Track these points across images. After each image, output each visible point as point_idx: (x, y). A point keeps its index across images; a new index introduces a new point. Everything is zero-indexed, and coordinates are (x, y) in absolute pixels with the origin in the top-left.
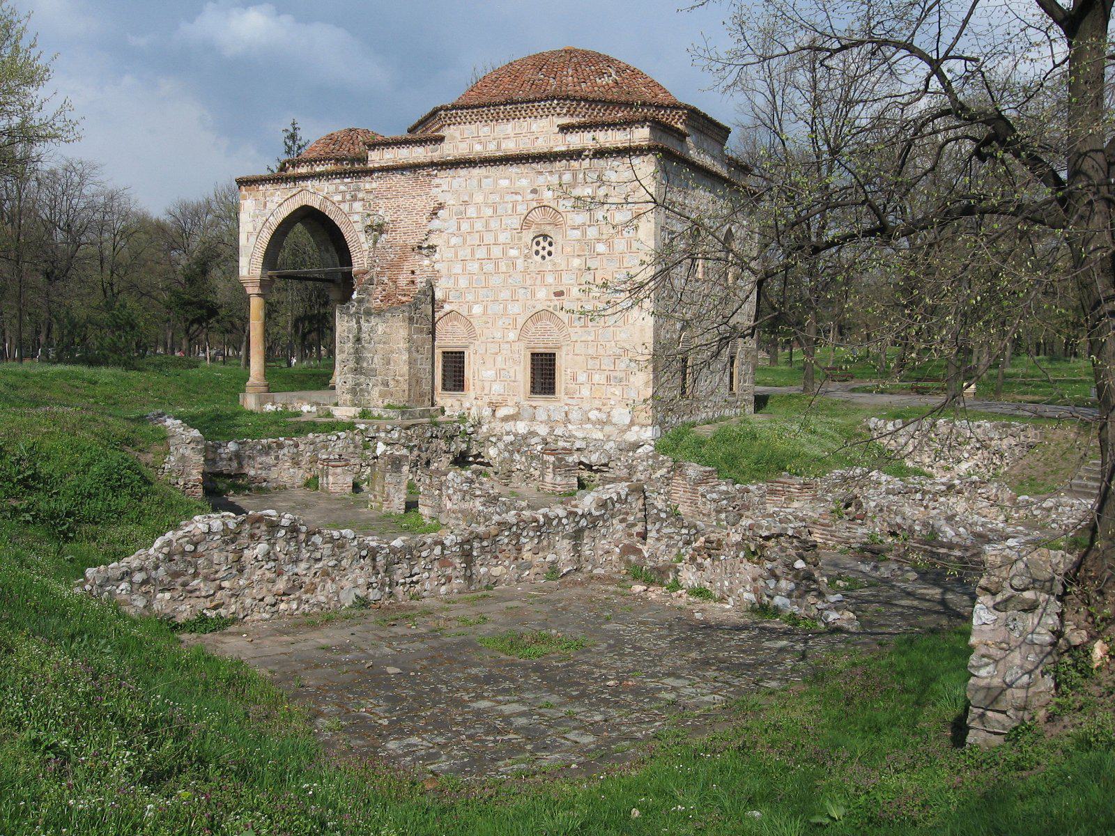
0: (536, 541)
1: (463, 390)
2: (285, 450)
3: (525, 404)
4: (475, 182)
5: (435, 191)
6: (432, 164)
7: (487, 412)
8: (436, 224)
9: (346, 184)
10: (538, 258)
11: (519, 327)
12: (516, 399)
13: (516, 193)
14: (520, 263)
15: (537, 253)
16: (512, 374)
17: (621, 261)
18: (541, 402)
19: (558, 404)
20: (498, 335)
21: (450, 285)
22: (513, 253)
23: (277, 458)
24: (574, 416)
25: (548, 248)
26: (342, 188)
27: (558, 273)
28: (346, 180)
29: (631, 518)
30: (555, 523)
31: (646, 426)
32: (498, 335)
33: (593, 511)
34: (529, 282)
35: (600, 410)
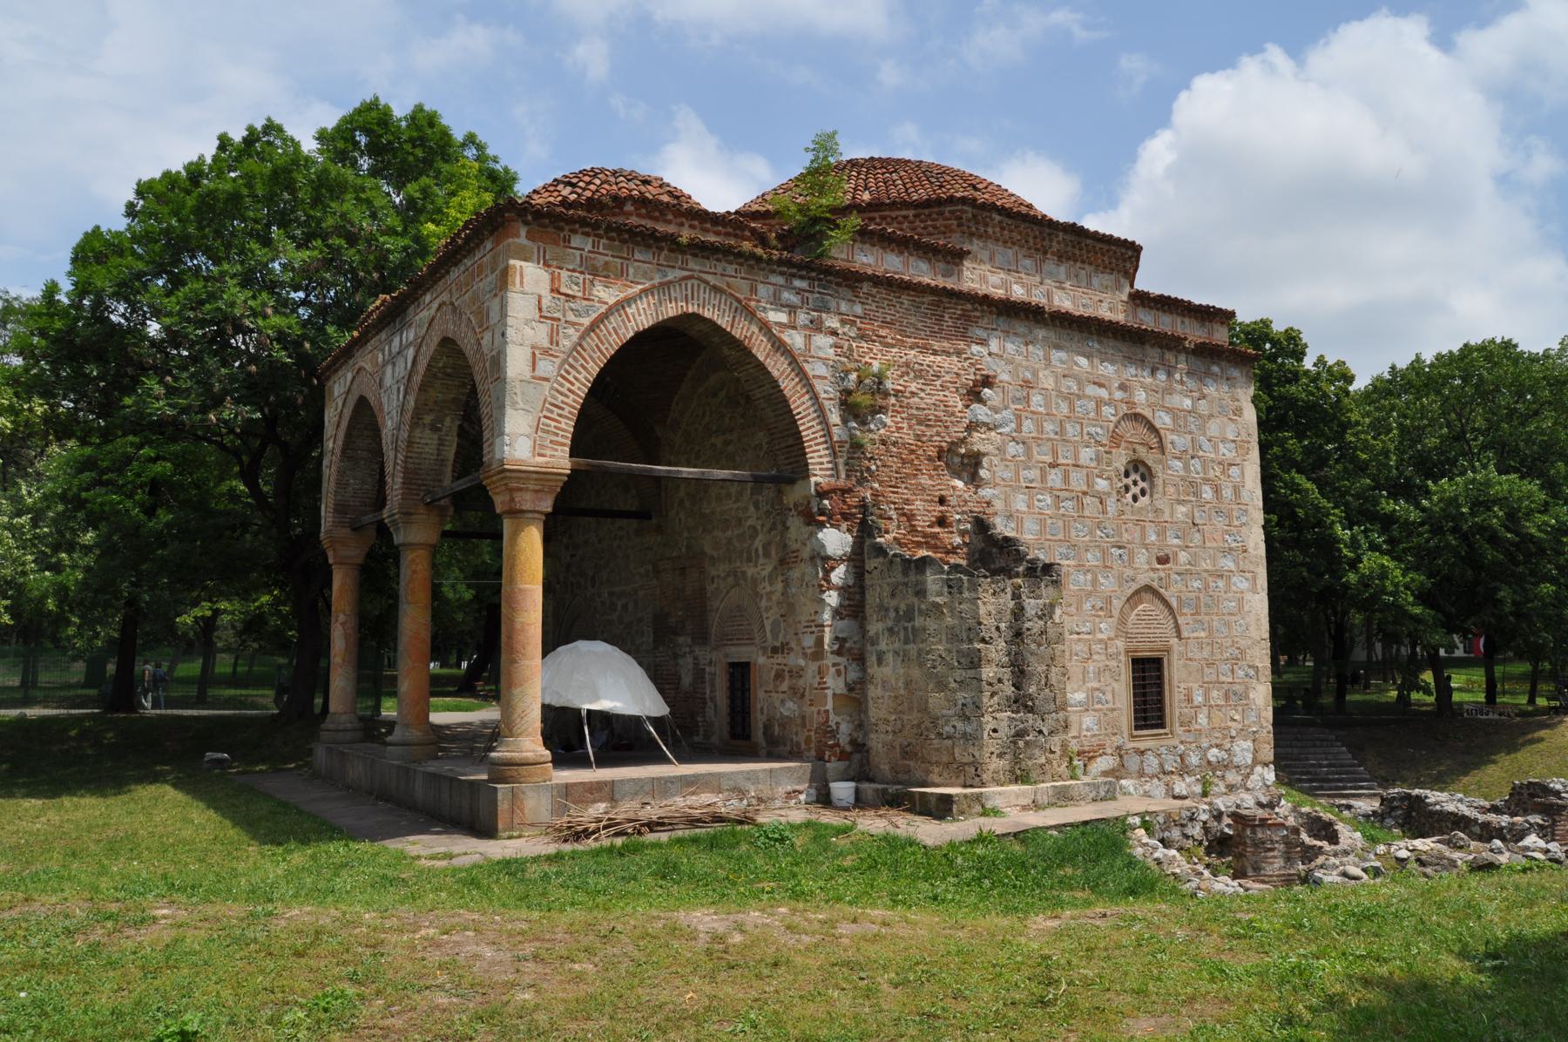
8: (980, 412)
9: (799, 291)
10: (1129, 496)
11: (1116, 613)
12: (1118, 741)
13: (1101, 385)
15: (1127, 489)
16: (1109, 697)
25: (1142, 484)
28: (797, 283)
34: (1126, 536)
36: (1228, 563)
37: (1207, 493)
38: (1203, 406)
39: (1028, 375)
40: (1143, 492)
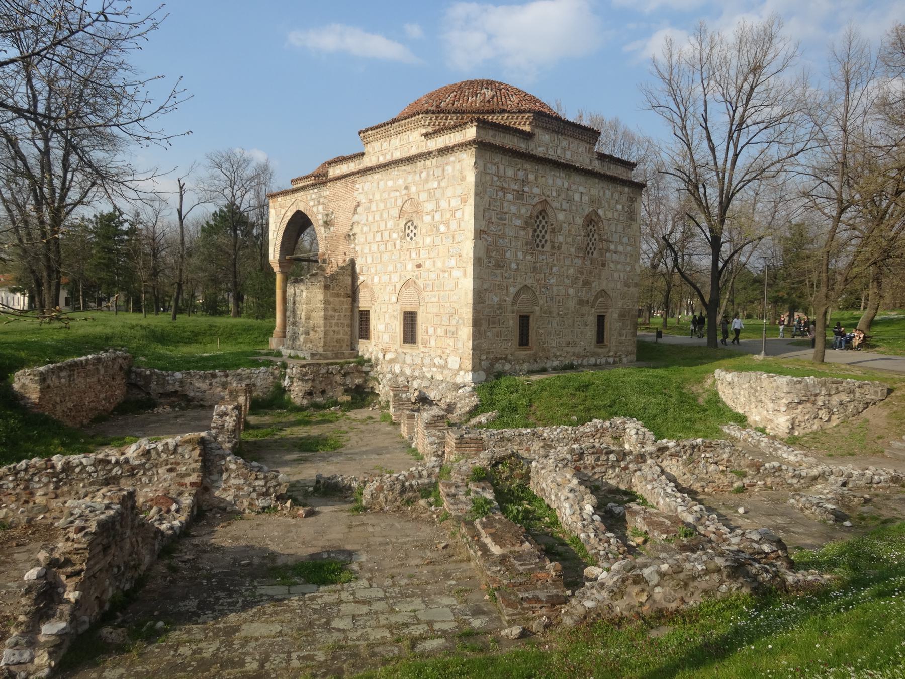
0: (52, 486)
1: (368, 339)
2: (218, 380)
3: (400, 350)
4: (375, 184)
5: (356, 193)
6: (353, 174)
7: (380, 356)
8: (356, 218)
10: (408, 239)
14: (398, 242)
15: (408, 235)
17: (454, 238)
18: (408, 348)
19: (418, 351)
20: (387, 298)
21: (363, 262)
22: (395, 236)
23: (211, 384)
24: (427, 361)
26: (314, 196)
27: (418, 249)
28: (316, 190)
29: (182, 469)
30: (77, 470)
31: (468, 371)
32: (387, 298)
33: (131, 460)
35: (441, 357)
36: (452, 262)
37: (442, 228)
38: (443, 184)
39: (371, 197)
40: (415, 235)
